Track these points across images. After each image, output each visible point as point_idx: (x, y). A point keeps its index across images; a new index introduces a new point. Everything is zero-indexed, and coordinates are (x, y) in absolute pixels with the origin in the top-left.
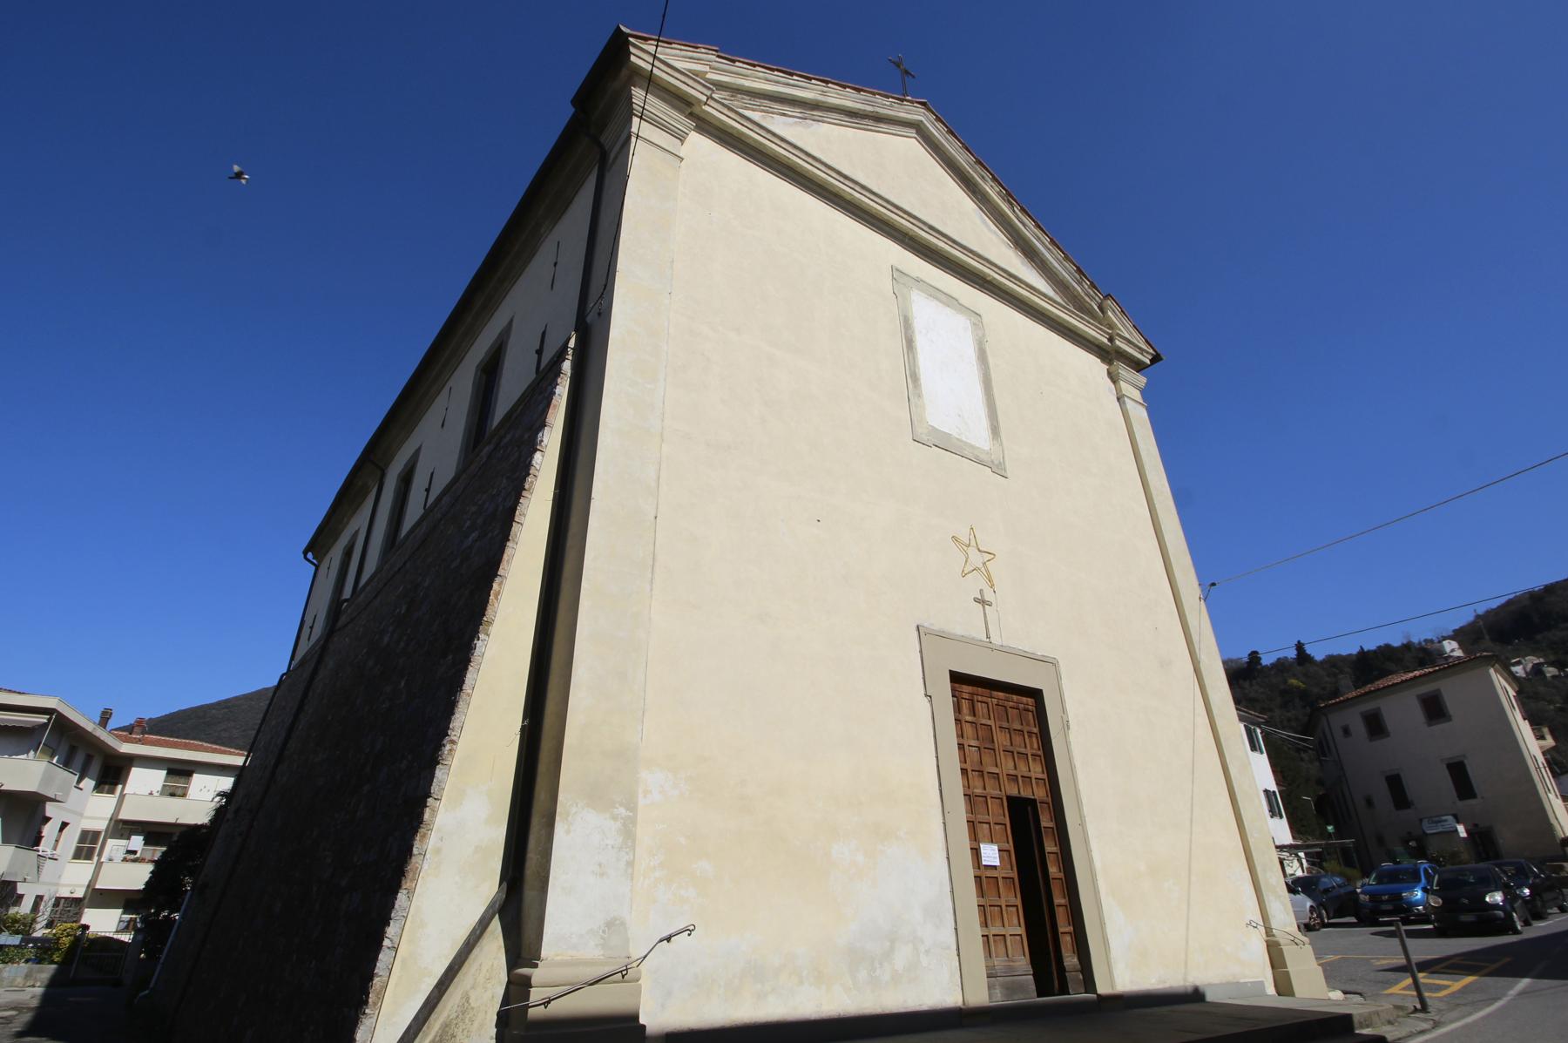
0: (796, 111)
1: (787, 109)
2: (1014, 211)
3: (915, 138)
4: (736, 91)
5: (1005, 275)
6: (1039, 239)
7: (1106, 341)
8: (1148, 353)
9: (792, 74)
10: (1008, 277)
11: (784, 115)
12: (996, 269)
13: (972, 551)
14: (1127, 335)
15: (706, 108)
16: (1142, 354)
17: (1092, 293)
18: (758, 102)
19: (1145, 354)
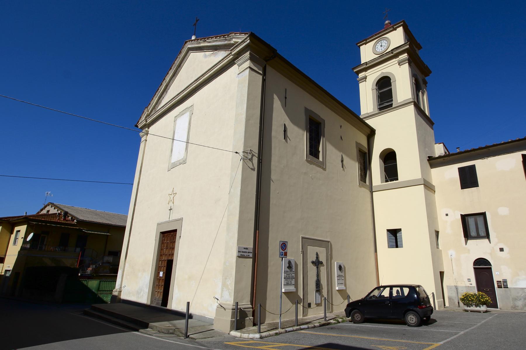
0: (165, 93)
1: (163, 96)
2: (207, 42)
3: (191, 53)
4: (154, 108)
5: (196, 82)
6: (214, 41)
7: (231, 57)
8: (246, 39)
9: (158, 89)
10: (197, 81)
11: (163, 98)
12: (193, 84)
13: (173, 195)
14: (240, 41)
15: (148, 122)
16: (245, 42)
17: (229, 38)
18: (158, 103)
19: (246, 41)
